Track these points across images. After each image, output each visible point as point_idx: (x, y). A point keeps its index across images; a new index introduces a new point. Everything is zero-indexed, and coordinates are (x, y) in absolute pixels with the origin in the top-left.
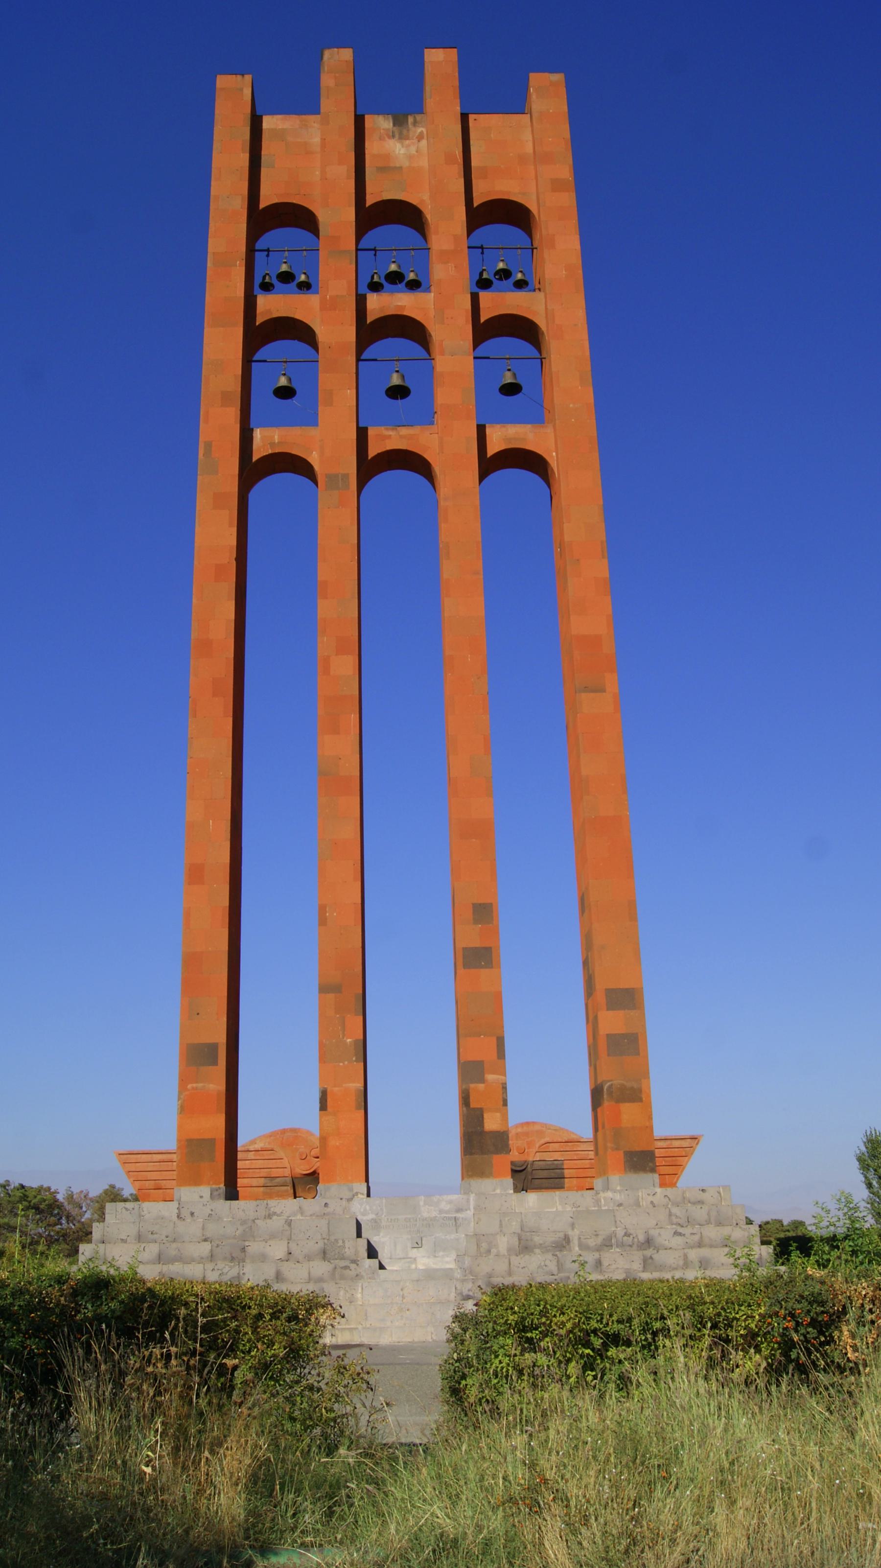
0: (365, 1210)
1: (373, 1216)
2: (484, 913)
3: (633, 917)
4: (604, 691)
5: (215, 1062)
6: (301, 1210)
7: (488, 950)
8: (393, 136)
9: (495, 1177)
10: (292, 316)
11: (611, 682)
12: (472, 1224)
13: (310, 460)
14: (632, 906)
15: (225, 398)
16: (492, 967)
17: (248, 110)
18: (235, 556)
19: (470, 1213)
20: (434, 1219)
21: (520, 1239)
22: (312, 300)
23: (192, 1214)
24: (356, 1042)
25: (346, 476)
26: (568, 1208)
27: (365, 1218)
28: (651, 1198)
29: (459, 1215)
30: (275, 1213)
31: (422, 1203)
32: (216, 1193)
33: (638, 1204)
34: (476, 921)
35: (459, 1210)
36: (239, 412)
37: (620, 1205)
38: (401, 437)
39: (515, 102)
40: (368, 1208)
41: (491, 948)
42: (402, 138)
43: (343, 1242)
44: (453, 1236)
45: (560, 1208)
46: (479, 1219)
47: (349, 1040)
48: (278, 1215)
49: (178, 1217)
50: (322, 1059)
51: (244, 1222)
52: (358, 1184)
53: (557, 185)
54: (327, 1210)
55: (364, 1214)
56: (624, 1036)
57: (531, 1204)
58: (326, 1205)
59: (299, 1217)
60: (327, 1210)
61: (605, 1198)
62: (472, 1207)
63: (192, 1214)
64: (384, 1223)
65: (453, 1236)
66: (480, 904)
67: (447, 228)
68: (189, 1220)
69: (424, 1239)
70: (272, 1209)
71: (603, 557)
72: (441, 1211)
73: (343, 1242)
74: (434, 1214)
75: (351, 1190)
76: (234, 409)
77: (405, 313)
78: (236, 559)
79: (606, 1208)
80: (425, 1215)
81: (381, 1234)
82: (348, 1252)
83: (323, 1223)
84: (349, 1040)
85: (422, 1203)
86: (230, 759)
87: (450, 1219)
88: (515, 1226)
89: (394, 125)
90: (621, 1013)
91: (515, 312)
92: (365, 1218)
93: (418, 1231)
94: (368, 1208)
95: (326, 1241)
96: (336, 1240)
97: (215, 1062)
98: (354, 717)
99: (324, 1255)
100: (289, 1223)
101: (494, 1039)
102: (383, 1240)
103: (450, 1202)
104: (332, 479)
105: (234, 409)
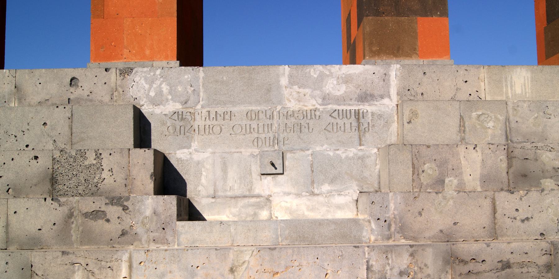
0: (160, 93)
1: (178, 107)
9: (423, 56)
12: (394, 127)
19: (389, 104)
20: (313, 114)
21: (510, 158)
27: (158, 110)
29: (365, 107)
31: (284, 81)
35: (365, 97)
40: (165, 88)
43: (98, 156)
44: (352, 152)
46: (415, 114)
54: (76, 93)
55: (155, 102)
57: (518, 90)
60: (76, 93)
62: (393, 91)
64: (199, 122)
65: (352, 152)
69: (288, 156)
72: (326, 99)
73: (98, 156)
74: (311, 104)
80: (292, 105)
81: (195, 145)
82: (109, 180)
83: (59, 117)
85: (284, 81)
87: (344, 114)
88: (493, 128)
92: (158, 110)
93: (276, 140)
94: (165, 88)
95: (57, 154)
96: (82, 154)
99: (52, 185)
102: (197, 157)
103: (347, 80)
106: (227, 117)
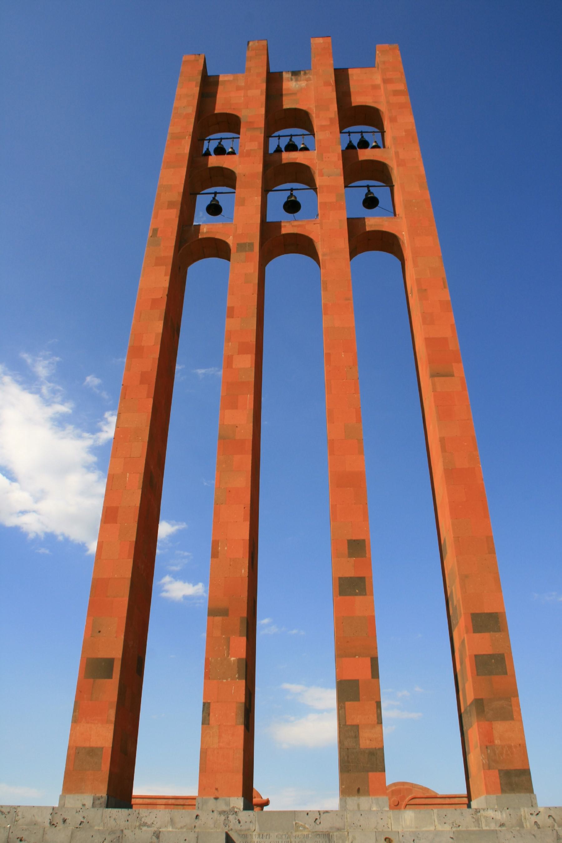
2: (357, 548)
3: (492, 551)
4: (453, 376)
5: (110, 676)
6: (172, 822)
7: (362, 580)
8: (292, 80)
10: (221, 165)
11: (459, 370)
13: (227, 241)
14: (489, 540)
15: (171, 205)
16: (366, 595)
17: (201, 68)
18: (167, 293)
22: (235, 158)
23: (64, 821)
24: (239, 660)
25: (251, 245)
26: (447, 828)
28: (534, 818)
30: (145, 824)
32: (98, 802)
33: (521, 825)
34: (351, 555)
36: (179, 212)
37: (502, 825)
38: (293, 226)
39: (369, 62)
41: (364, 578)
42: (297, 80)
45: (439, 828)
47: (232, 659)
48: (149, 826)
49: (50, 823)
50: (207, 676)
51: (112, 832)
52: (236, 798)
53: (396, 93)
56: (491, 656)
58: (197, 816)
59: (170, 829)
60: (198, 823)
61: (486, 817)
63: (64, 821)
66: (354, 541)
67: (325, 117)
68: (61, 826)
70: (143, 820)
71: (445, 287)
75: (228, 804)
76: (175, 210)
77: (298, 161)
78: (167, 295)
79: (487, 828)
84: (232, 659)
86: (149, 428)
89: (292, 75)
90: (487, 635)
91: (372, 158)
97: (110, 676)
98: (250, 398)
100: (157, 835)
101: (368, 661)
104: (242, 247)
105: (175, 210)
106: (268, 837)
